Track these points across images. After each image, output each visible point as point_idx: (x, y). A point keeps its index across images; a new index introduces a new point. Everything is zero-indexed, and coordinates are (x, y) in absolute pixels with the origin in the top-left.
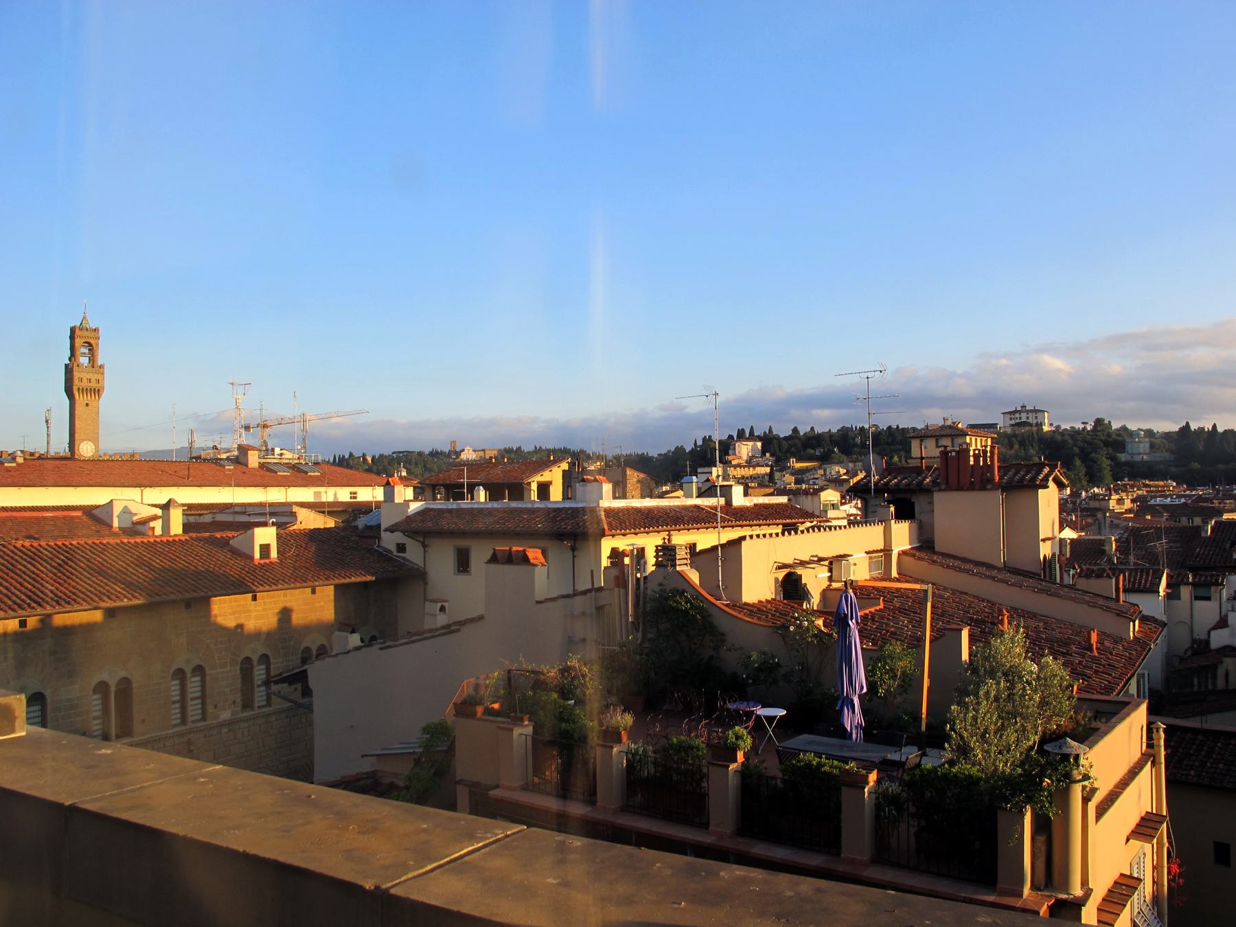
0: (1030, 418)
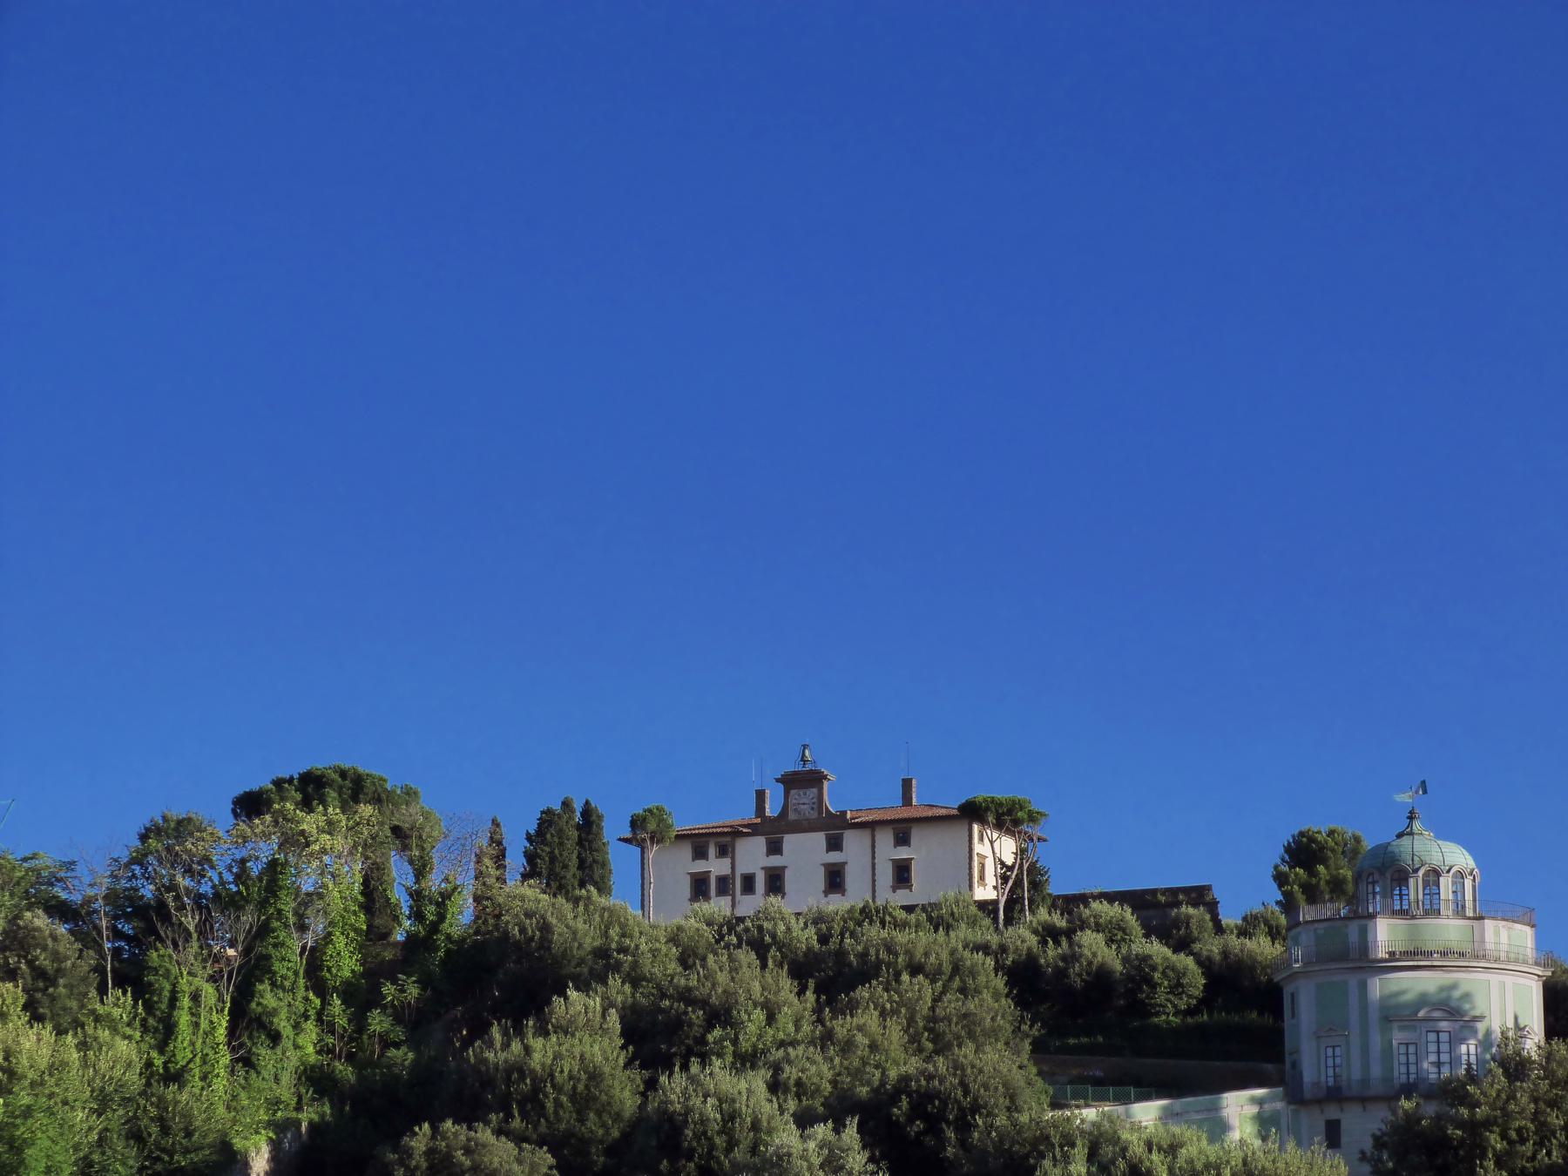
0: (856, 879)
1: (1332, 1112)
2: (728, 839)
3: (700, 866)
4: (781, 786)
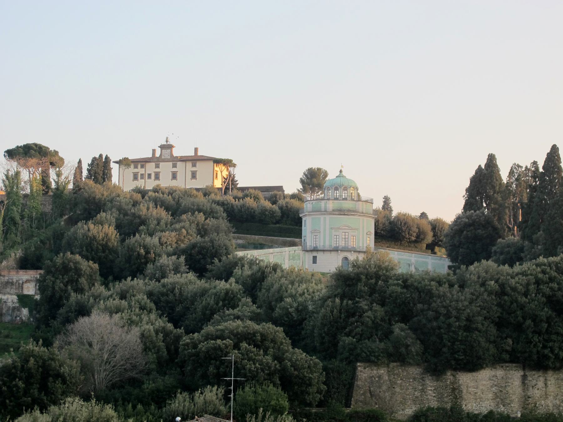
1: (315, 254)
2: (144, 163)
3: (136, 170)
4: (160, 149)
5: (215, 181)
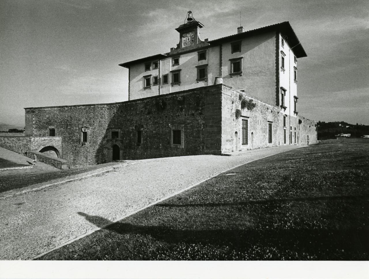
5: (281, 73)
